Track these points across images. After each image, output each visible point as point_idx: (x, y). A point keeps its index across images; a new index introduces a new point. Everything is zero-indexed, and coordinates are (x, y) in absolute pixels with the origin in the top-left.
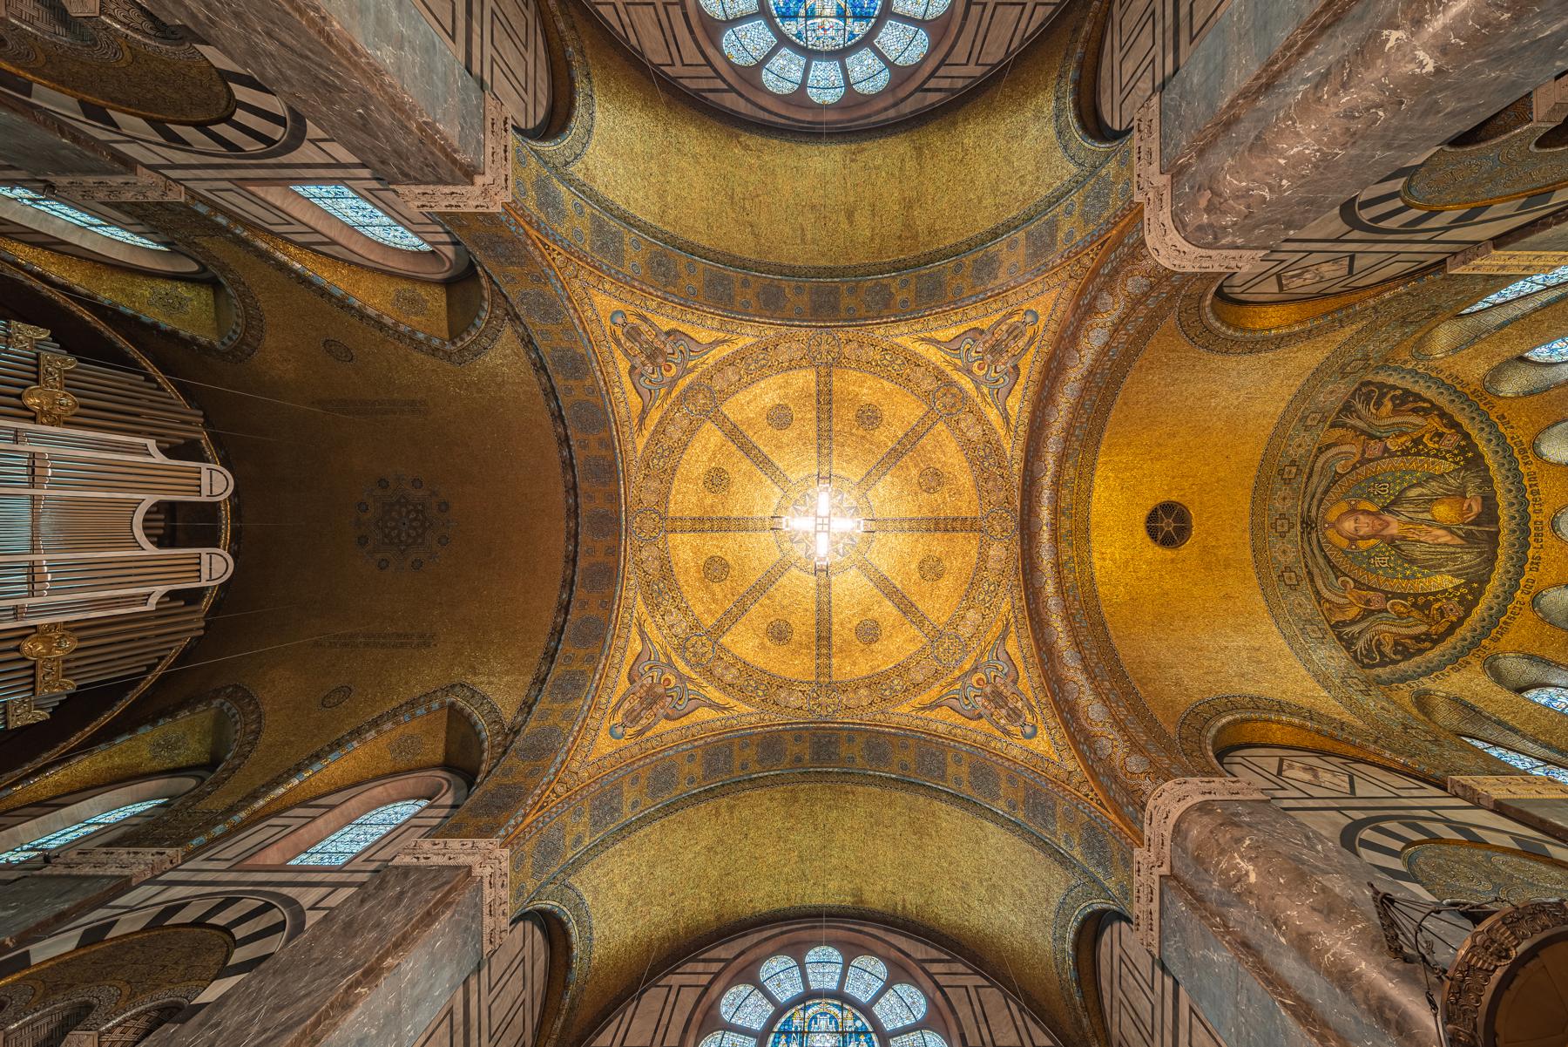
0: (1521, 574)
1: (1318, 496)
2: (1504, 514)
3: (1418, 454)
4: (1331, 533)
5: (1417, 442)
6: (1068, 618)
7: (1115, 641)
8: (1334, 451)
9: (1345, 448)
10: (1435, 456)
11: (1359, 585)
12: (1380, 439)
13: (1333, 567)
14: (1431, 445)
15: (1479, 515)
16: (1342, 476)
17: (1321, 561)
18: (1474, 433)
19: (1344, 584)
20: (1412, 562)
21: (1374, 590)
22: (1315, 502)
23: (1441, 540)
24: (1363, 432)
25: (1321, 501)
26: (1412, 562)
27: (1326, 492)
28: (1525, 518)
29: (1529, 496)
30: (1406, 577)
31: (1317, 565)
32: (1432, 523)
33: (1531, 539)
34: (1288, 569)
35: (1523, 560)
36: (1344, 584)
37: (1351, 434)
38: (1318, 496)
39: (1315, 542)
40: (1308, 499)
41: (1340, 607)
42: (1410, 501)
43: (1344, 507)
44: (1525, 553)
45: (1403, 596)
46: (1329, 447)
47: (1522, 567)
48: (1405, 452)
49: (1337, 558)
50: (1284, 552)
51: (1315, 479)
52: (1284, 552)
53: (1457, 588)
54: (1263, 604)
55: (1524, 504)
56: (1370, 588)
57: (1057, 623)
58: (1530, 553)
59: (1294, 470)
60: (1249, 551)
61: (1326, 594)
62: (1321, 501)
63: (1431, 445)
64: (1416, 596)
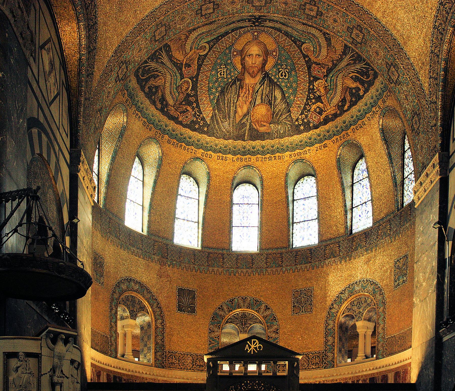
0: (215, 151)
2: (258, 143)
3: (308, 99)
5: (318, 99)
8: (324, 43)
9: (324, 52)
10: (305, 108)
11: (202, 59)
12: (327, 76)
14: (314, 107)
15: (257, 131)
18: (317, 131)
19: (203, 48)
20: (222, 92)
21: (199, 69)
23: (239, 110)
24: (335, 65)
26: (222, 92)
29: (268, 156)
30: (210, 89)
32: (253, 104)
33: (239, 156)
35: (225, 152)
36: (203, 48)
37: (336, 57)
41: (182, 47)
44: (229, 153)
45: (194, 88)
46: (328, 40)
47: (220, 152)
48: (311, 90)
53: (203, 119)
55: (263, 153)
56: (199, 66)
58: (230, 156)
59: (313, 13)
63: (314, 107)
64: (196, 96)
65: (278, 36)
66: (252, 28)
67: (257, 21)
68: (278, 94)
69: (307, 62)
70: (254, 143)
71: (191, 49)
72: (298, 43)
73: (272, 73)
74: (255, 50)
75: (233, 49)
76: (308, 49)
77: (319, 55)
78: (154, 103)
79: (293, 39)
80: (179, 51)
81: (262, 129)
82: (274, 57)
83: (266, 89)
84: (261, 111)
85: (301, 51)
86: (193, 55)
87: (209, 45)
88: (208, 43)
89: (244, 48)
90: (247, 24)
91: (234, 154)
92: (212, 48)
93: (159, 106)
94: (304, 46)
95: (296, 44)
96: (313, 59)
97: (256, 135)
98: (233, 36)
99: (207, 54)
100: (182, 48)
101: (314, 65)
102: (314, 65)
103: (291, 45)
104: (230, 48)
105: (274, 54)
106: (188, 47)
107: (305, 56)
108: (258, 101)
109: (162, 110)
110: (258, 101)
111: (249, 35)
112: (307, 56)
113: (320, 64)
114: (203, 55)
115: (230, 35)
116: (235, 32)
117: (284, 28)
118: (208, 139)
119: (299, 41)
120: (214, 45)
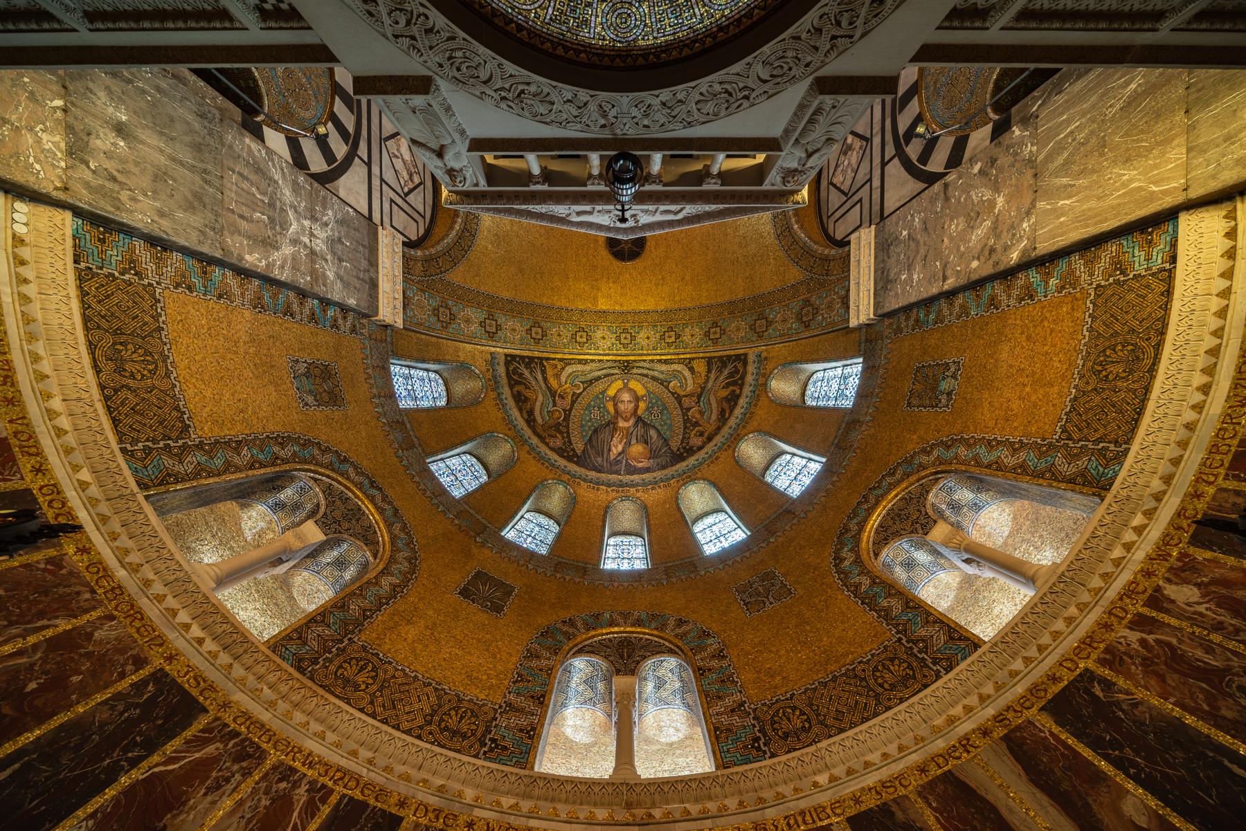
1: (651, 373)
4: (619, 384)
13: (591, 382)
16: (667, 387)
17: (599, 373)
22: (645, 372)
25: (646, 376)
27: (654, 378)
28: (633, 486)
38: (651, 373)
42: (646, 432)
43: (641, 391)
49: (600, 386)
51: (664, 368)
68: (652, 433)
70: (632, 477)
73: (645, 416)
74: (626, 397)
78: (520, 410)
81: (640, 465)
83: (640, 430)
84: (637, 449)
91: (609, 485)
93: (526, 416)
97: (632, 470)
104: (603, 392)
108: (634, 441)
109: (528, 422)
110: (634, 441)
111: (620, 382)
118: (577, 469)
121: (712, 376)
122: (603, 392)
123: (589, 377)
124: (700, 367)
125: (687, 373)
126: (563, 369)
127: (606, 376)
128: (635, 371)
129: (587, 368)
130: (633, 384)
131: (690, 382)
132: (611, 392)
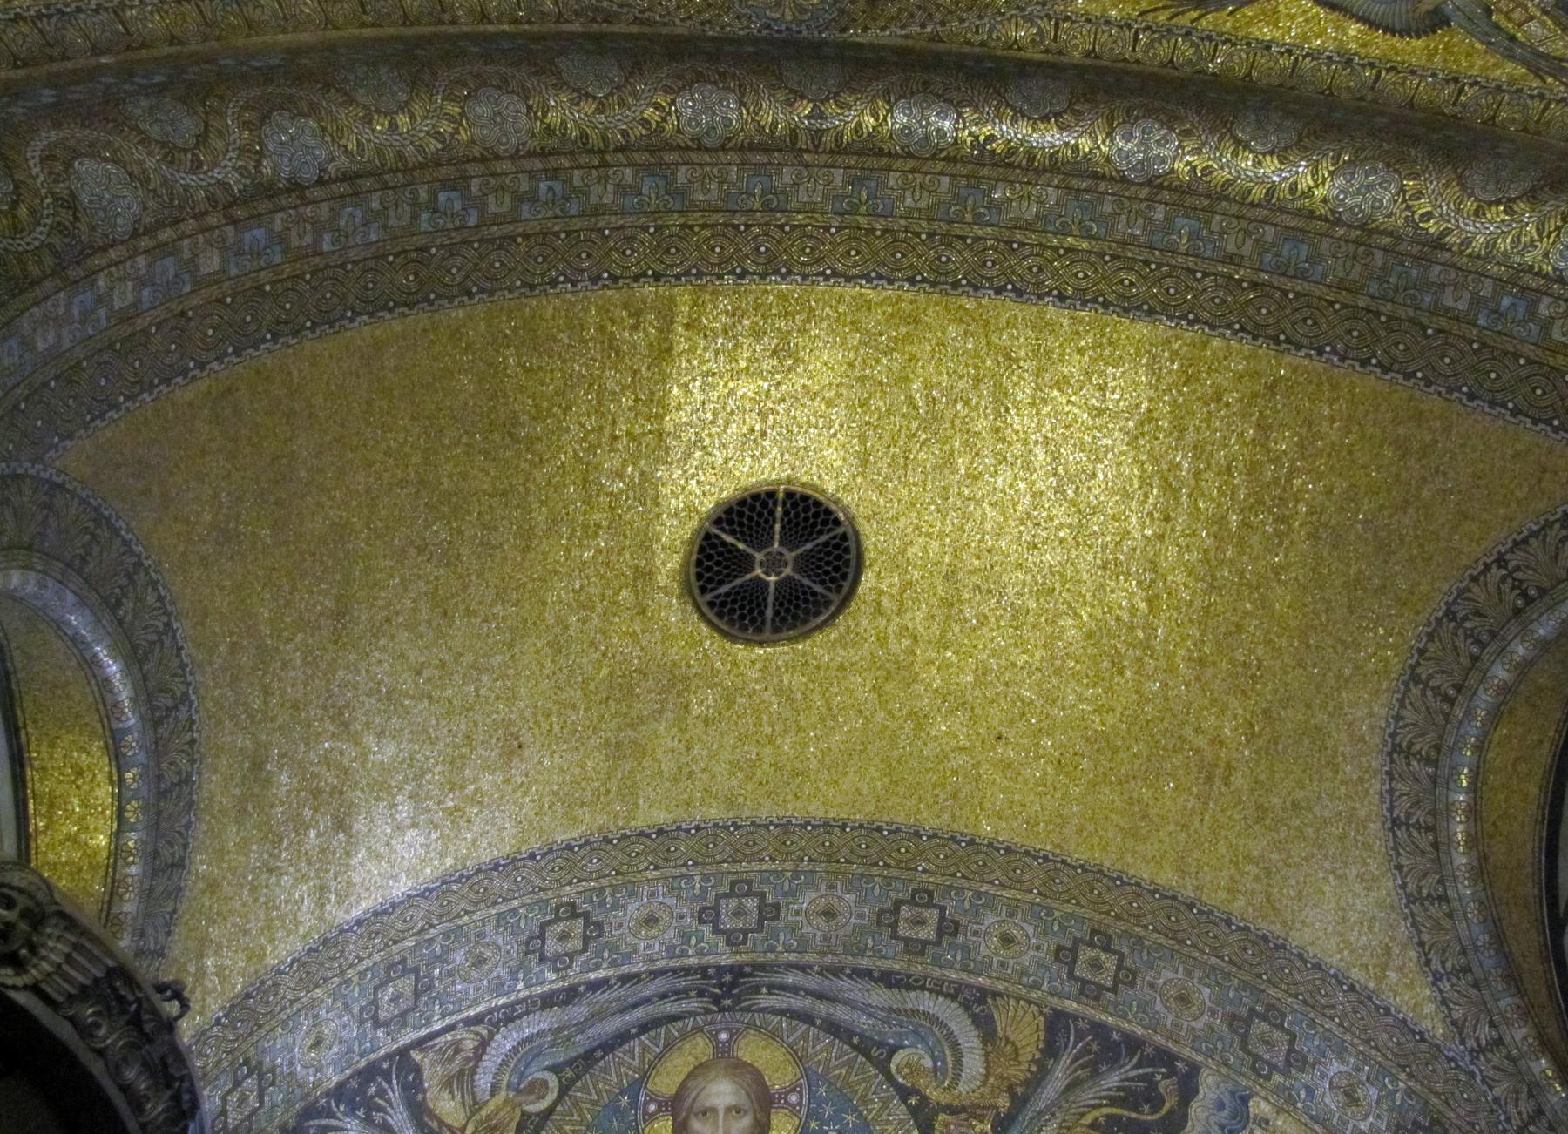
6: (453, 167)
7: (362, 332)
13: (588, 1058)
19: (537, 1088)
25: (807, 1018)
27: (834, 1028)
31: (598, 1016)
34: (594, 930)
36: (537, 1088)
39: (669, 1008)
40: (813, 982)
49: (617, 1070)
50: (651, 921)
51: (880, 997)
52: (651, 921)
54: (486, 855)
57: (417, 125)
60: (661, 817)
61: (505, 1041)
62: (807, 1018)
65: (805, 1037)
66: (709, 1017)
67: (729, 989)
69: (913, 1111)
71: (494, 1090)
72: (874, 1052)
75: (643, 1092)
76: (914, 1069)
77: (956, 1078)
79: (855, 1041)
80: (451, 1092)
82: (793, 1110)
85: (890, 1078)
86: (498, 1110)
87: (559, 1079)
88: (554, 1069)
89: (683, 1087)
90: (694, 1005)
92: (568, 1088)
94: (898, 1058)
95: (867, 1055)
96: (934, 1094)
98: (645, 1048)
99: (550, 1111)
100: (460, 1083)
101: (942, 1117)
102: (942, 1117)
103: (850, 1064)
104: (634, 1088)
105: (793, 1098)
106: (483, 1081)
107: (904, 1093)
112: (915, 1091)
113: (963, 1109)
114: (537, 1114)
115: (635, 1043)
116: (653, 1033)
117: (822, 1008)
119: (880, 1044)
120: (578, 1077)
121: (1060, 1075)
122: (634, 1088)
123: (582, 1042)
124: (1025, 1033)
125: (969, 1038)
126: (484, 1044)
127: (644, 1028)
128: (765, 1000)
129: (579, 1011)
130: (753, 1050)
131: (974, 1063)
132: (665, 1082)
